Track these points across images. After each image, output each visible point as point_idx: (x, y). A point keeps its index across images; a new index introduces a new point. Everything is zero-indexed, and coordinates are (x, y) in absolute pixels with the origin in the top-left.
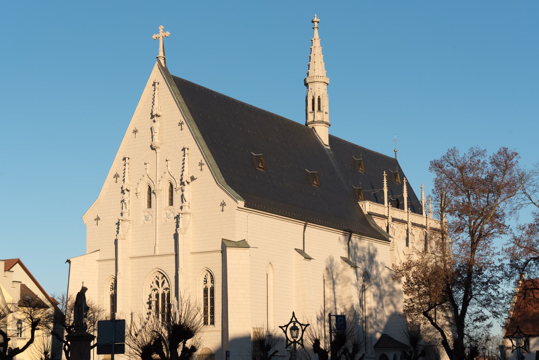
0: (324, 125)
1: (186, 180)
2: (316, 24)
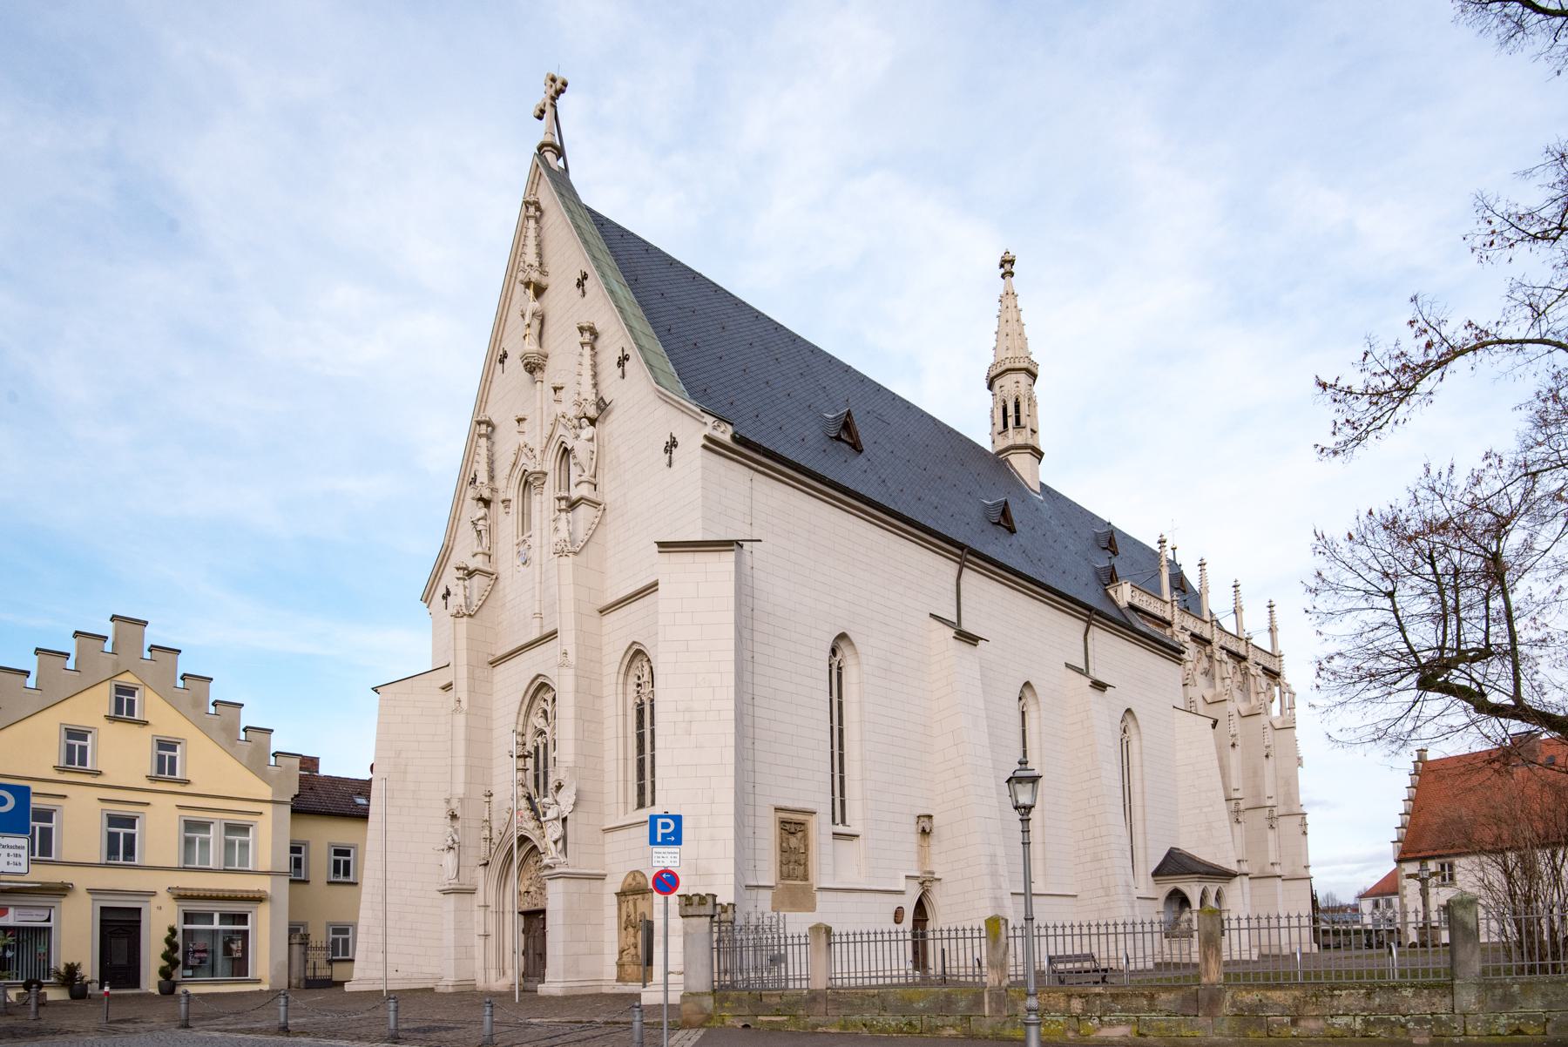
0: (1030, 451)
1: (585, 414)
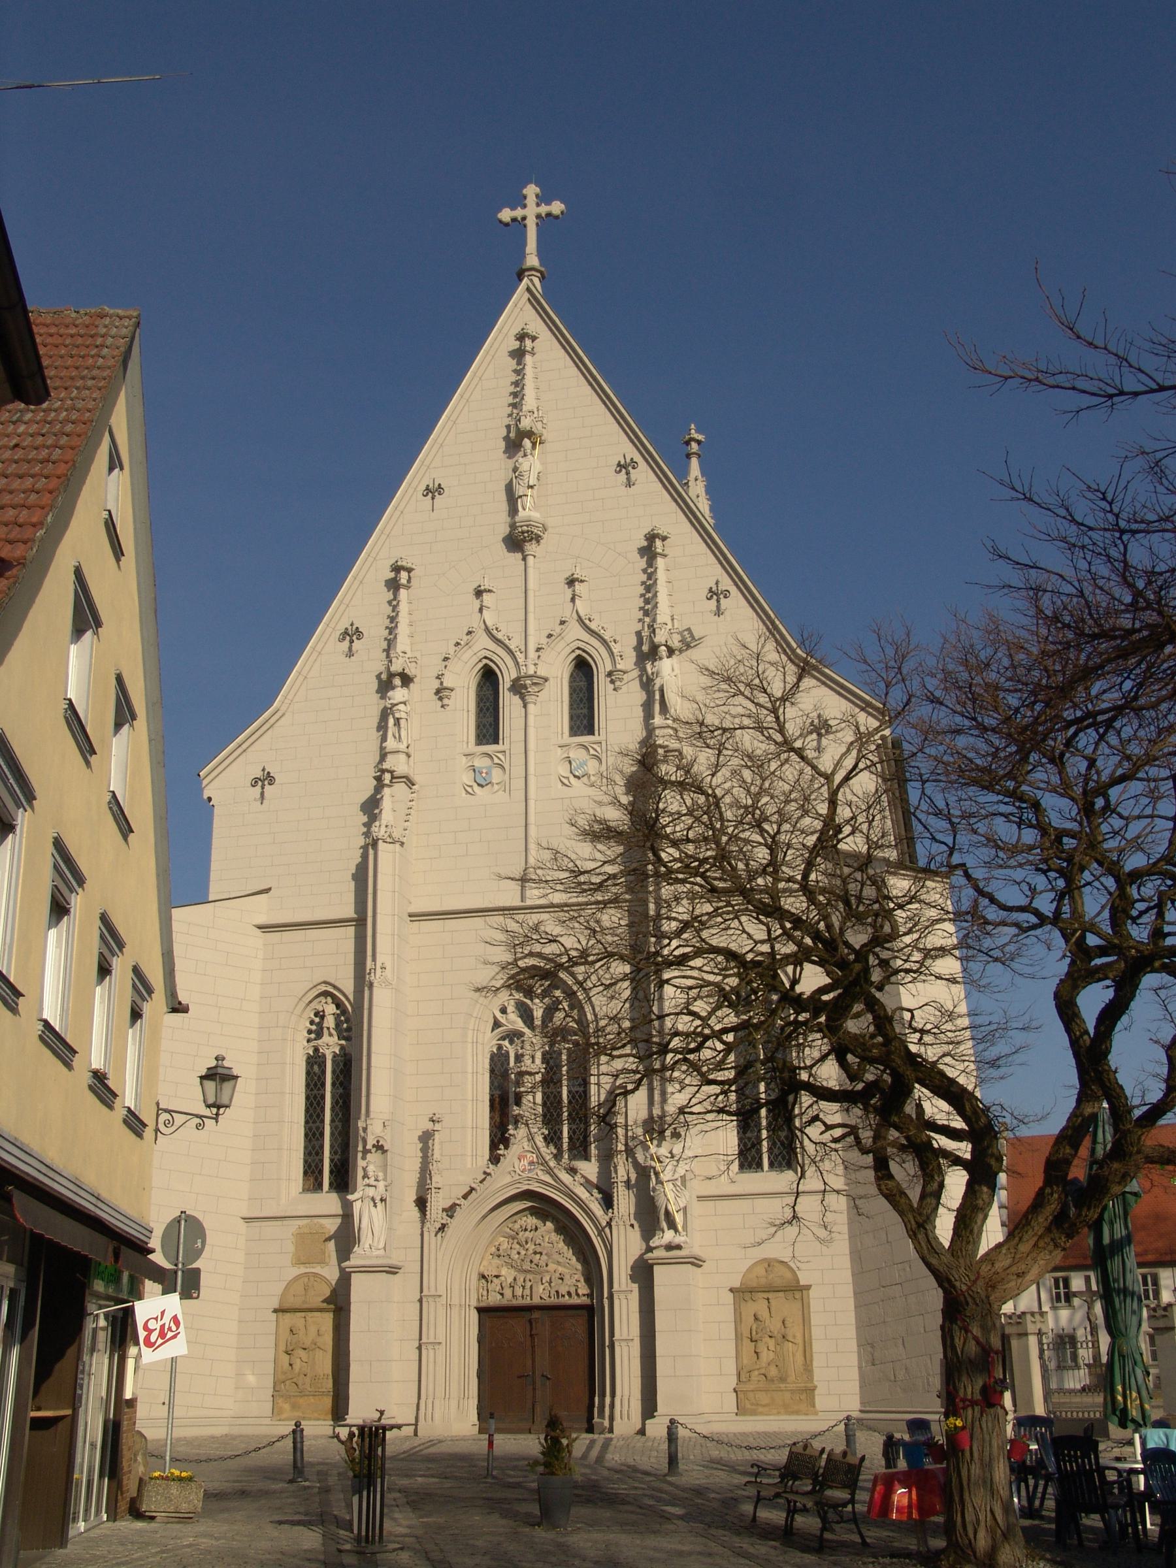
2: (694, 445)
